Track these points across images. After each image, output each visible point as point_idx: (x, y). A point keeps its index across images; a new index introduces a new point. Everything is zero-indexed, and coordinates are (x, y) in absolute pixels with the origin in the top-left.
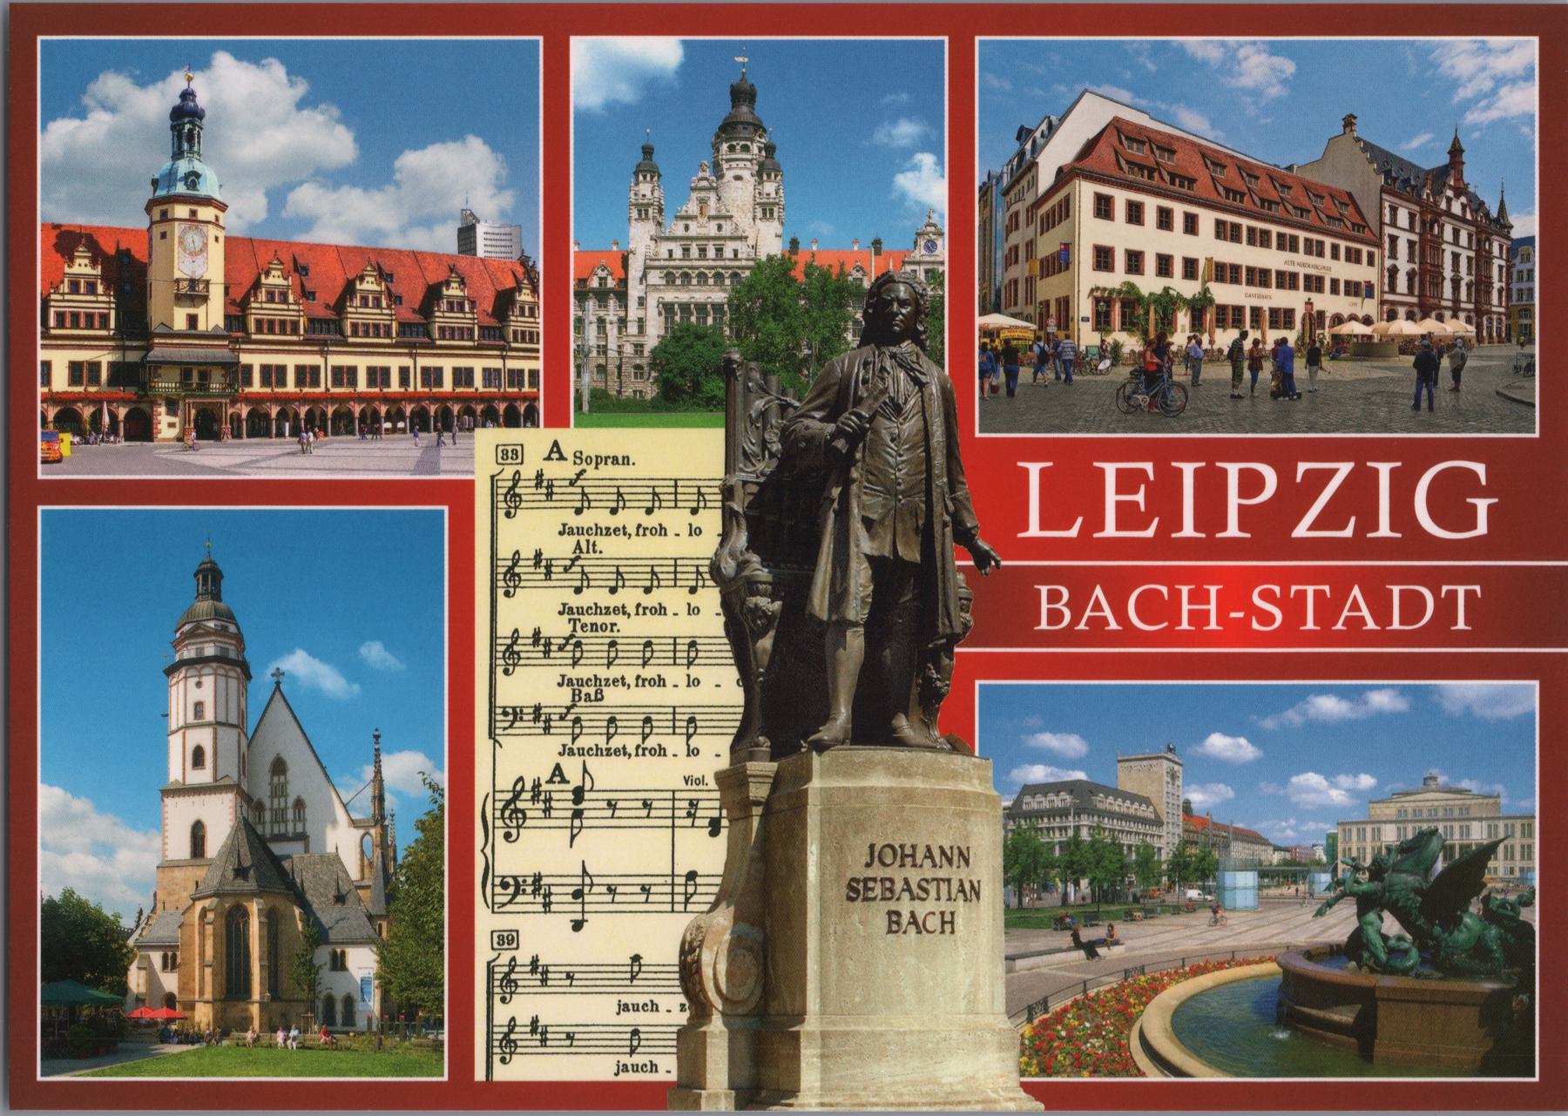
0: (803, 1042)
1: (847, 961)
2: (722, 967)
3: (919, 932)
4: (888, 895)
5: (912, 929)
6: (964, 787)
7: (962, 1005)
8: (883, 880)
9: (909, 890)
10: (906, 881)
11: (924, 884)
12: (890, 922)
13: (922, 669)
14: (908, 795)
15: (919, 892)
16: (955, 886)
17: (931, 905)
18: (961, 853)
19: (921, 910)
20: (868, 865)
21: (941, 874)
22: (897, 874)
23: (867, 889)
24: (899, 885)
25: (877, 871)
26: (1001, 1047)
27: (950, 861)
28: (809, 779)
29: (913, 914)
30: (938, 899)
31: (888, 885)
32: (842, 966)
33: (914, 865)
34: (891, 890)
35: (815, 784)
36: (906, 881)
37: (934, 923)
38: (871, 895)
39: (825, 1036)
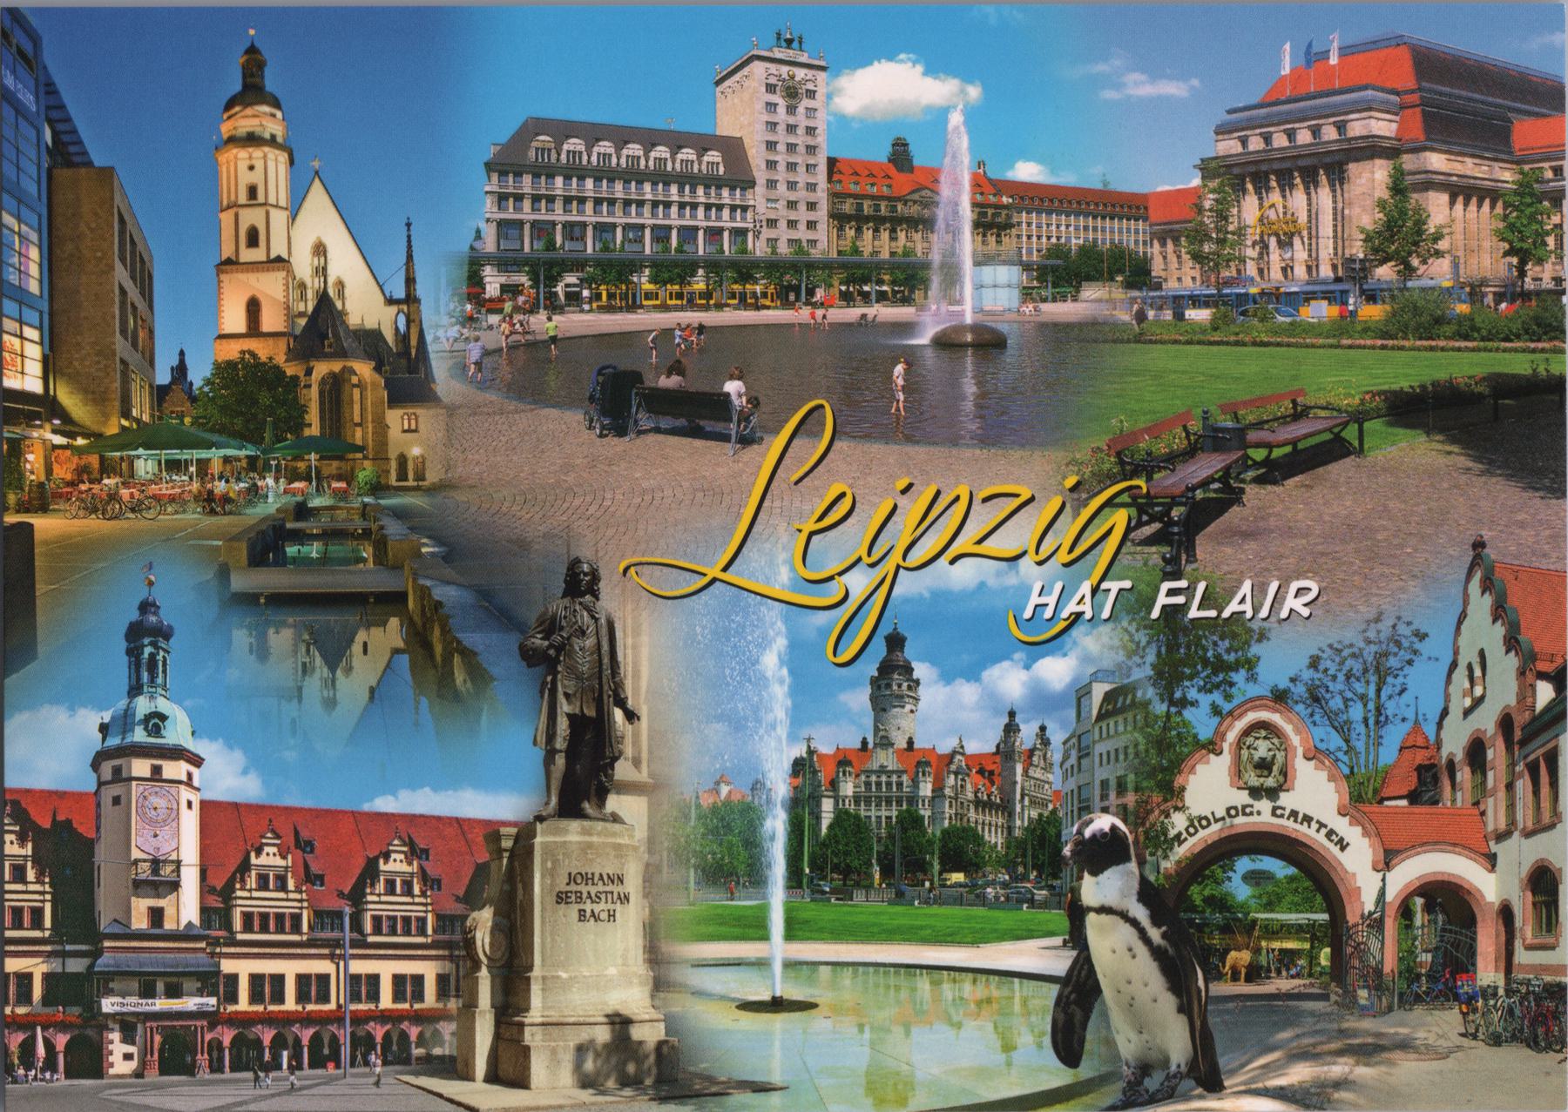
0: (532, 982)
2: (487, 940)
6: (619, 841)
7: (620, 961)
13: (598, 776)
14: (590, 845)
15: (595, 899)
17: (602, 906)
19: (597, 908)
21: (608, 889)
22: (584, 889)
24: (585, 895)
25: (573, 887)
26: (641, 984)
28: (534, 836)
35: (538, 840)
37: (604, 916)
39: (544, 978)
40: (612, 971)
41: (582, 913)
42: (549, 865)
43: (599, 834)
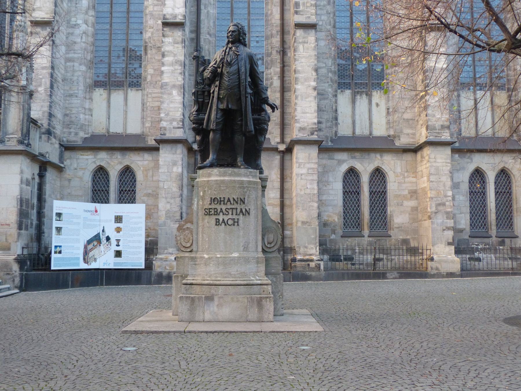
1: (204, 235)
3: (225, 225)
4: (216, 213)
5: (223, 224)
7: (242, 249)
8: (214, 209)
9: (222, 212)
10: (221, 209)
11: (227, 210)
12: (216, 222)
16: (239, 211)
17: (230, 216)
18: (241, 200)
19: (226, 218)
20: (210, 204)
21: (233, 207)
22: (218, 207)
23: (210, 212)
24: (219, 210)
25: (213, 206)
27: (237, 203)
29: (223, 220)
30: (232, 214)
31: (216, 210)
32: (202, 236)
33: (224, 204)
34: (217, 211)
36: (221, 209)
37: (230, 222)
38: (211, 213)
40: (235, 255)
41: (217, 221)
42: (201, 194)
43: (230, 175)
